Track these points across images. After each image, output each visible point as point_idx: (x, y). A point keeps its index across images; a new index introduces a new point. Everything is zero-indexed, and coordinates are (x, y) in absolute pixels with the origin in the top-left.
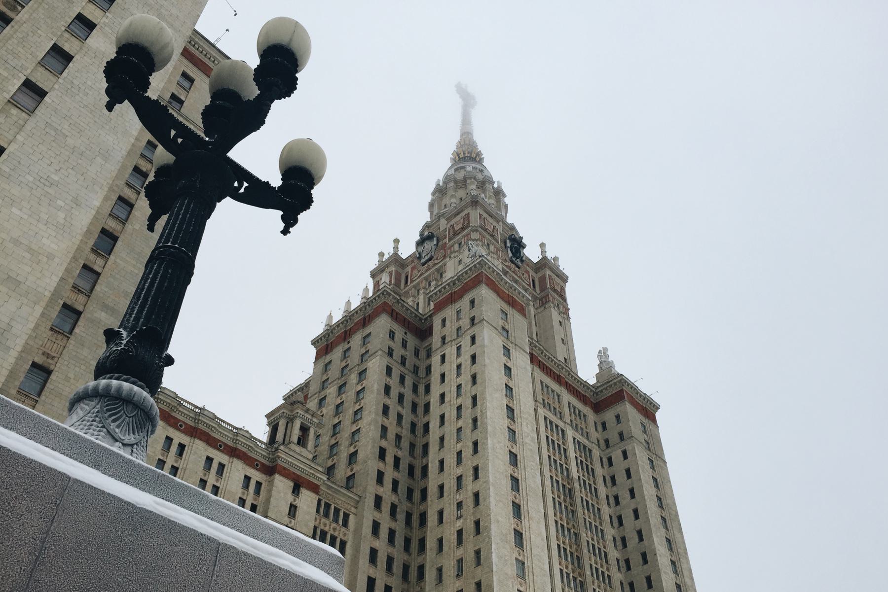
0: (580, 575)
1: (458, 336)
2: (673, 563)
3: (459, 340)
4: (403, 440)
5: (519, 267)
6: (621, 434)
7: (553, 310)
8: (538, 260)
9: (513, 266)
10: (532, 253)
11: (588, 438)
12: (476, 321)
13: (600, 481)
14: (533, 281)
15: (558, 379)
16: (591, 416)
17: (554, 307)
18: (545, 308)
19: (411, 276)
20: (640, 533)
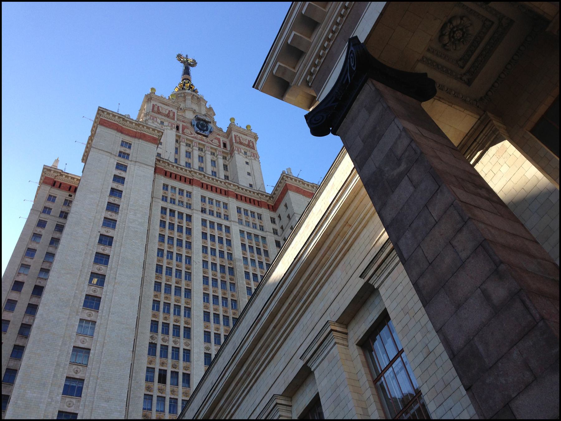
16: (266, 214)
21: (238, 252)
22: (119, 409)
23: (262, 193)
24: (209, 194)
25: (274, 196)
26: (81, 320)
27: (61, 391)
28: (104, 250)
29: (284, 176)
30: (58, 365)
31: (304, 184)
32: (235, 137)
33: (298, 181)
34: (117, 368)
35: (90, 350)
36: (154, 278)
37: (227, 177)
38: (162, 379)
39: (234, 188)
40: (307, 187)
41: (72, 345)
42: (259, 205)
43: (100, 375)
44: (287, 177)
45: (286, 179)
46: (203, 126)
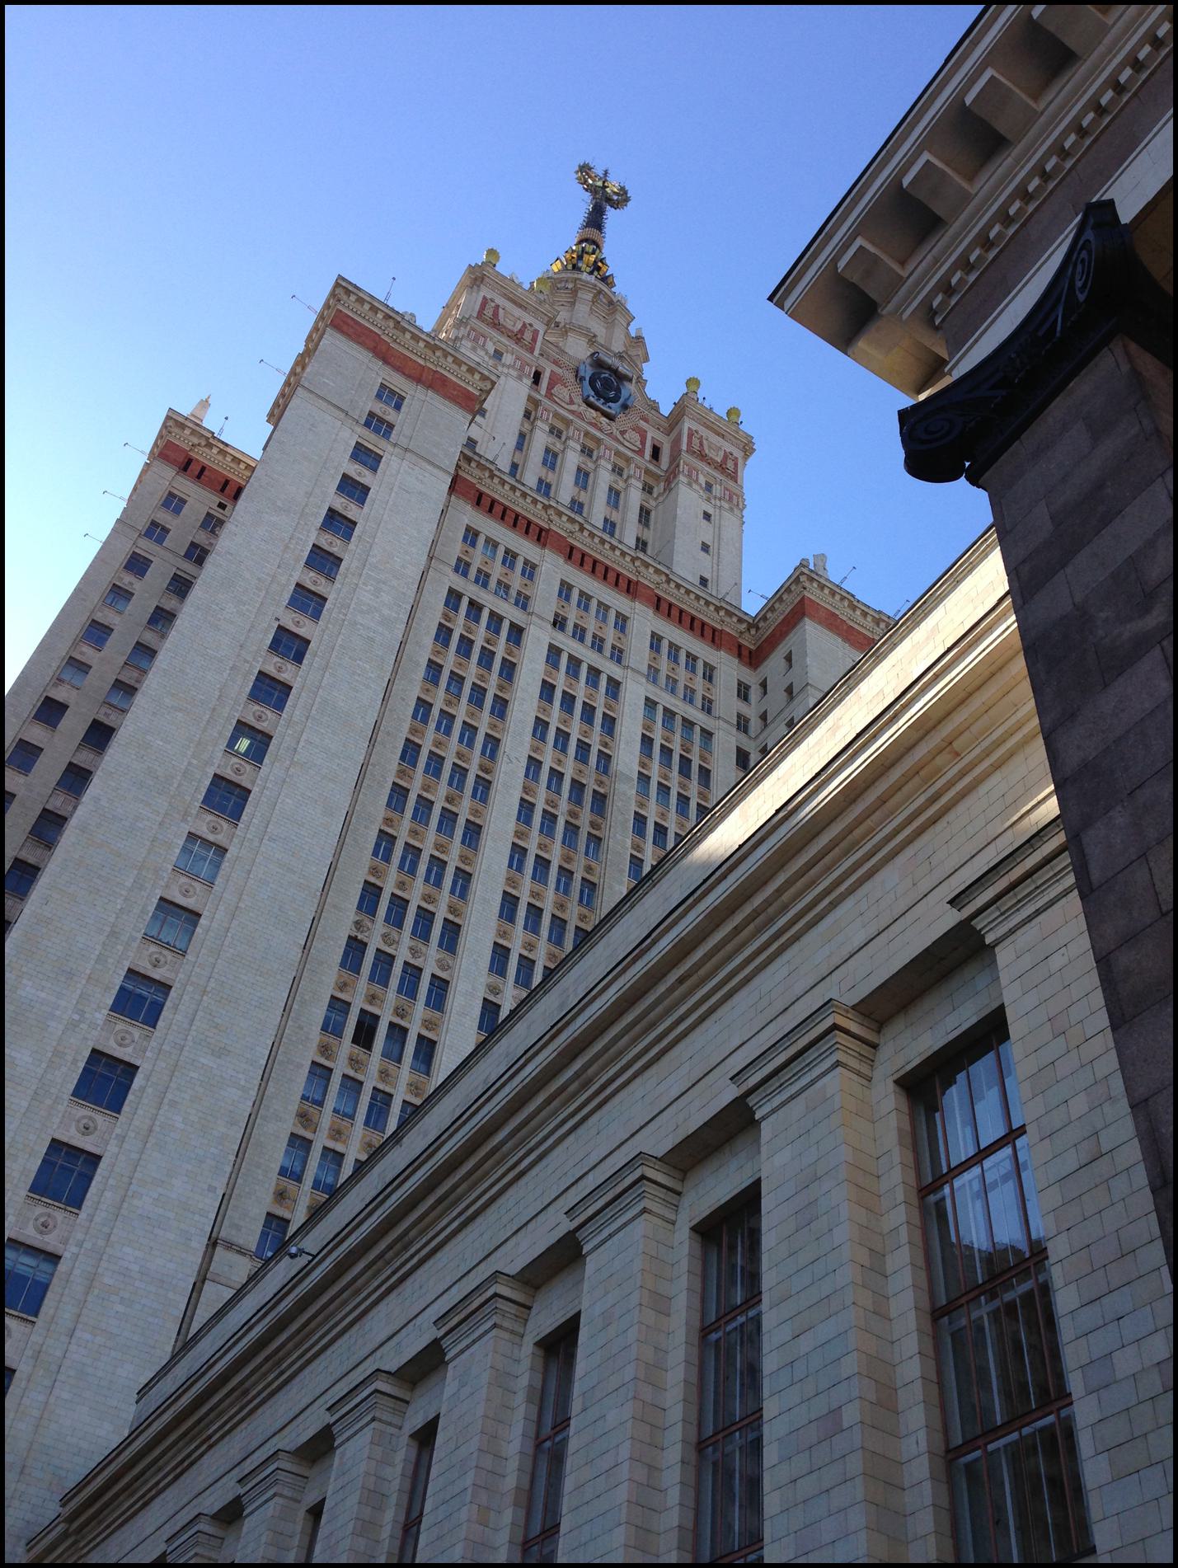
5: (611, 418)
16: (729, 669)
21: (627, 757)
22: (242, 1083)
23: (728, 608)
24: (582, 581)
25: (761, 624)
26: (192, 837)
27: (110, 1002)
28: (279, 670)
29: (803, 573)
30: (114, 934)
31: (854, 608)
32: (690, 435)
33: (837, 597)
34: (258, 978)
35: (199, 915)
36: (394, 772)
37: (642, 545)
38: (364, 1035)
39: (656, 578)
40: (860, 619)
41: (159, 893)
42: (713, 641)
43: (212, 984)
44: (812, 580)
45: (807, 584)
46: (607, 384)
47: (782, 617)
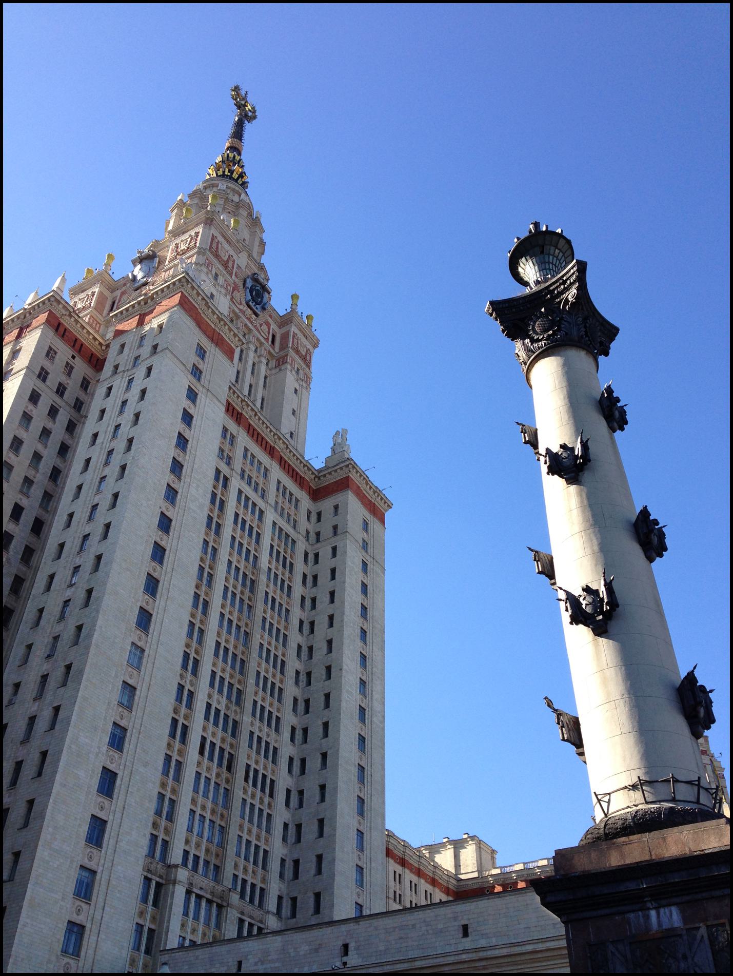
0: (239, 682)
1: (134, 365)
2: (363, 683)
3: (133, 371)
4: (34, 487)
5: (257, 315)
6: (335, 528)
7: (288, 373)
8: (285, 312)
9: (250, 312)
10: (279, 302)
11: (294, 527)
12: (159, 349)
13: (298, 579)
14: (274, 337)
15: (271, 451)
16: (306, 502)
17: (291, 371)
18: (280, 370)
19: (119, 301)
20: (330, 642)
21: (264, 560)
23: (310, 467)
24: (255, 449)
29: (351, 464)
31: (367, 484)
33: (362, 478)
40: (368, 490)
42: (300, 484)
43: (142, 728)
44: (354, 467)
45: (351, 470)
47: (334, 480)
